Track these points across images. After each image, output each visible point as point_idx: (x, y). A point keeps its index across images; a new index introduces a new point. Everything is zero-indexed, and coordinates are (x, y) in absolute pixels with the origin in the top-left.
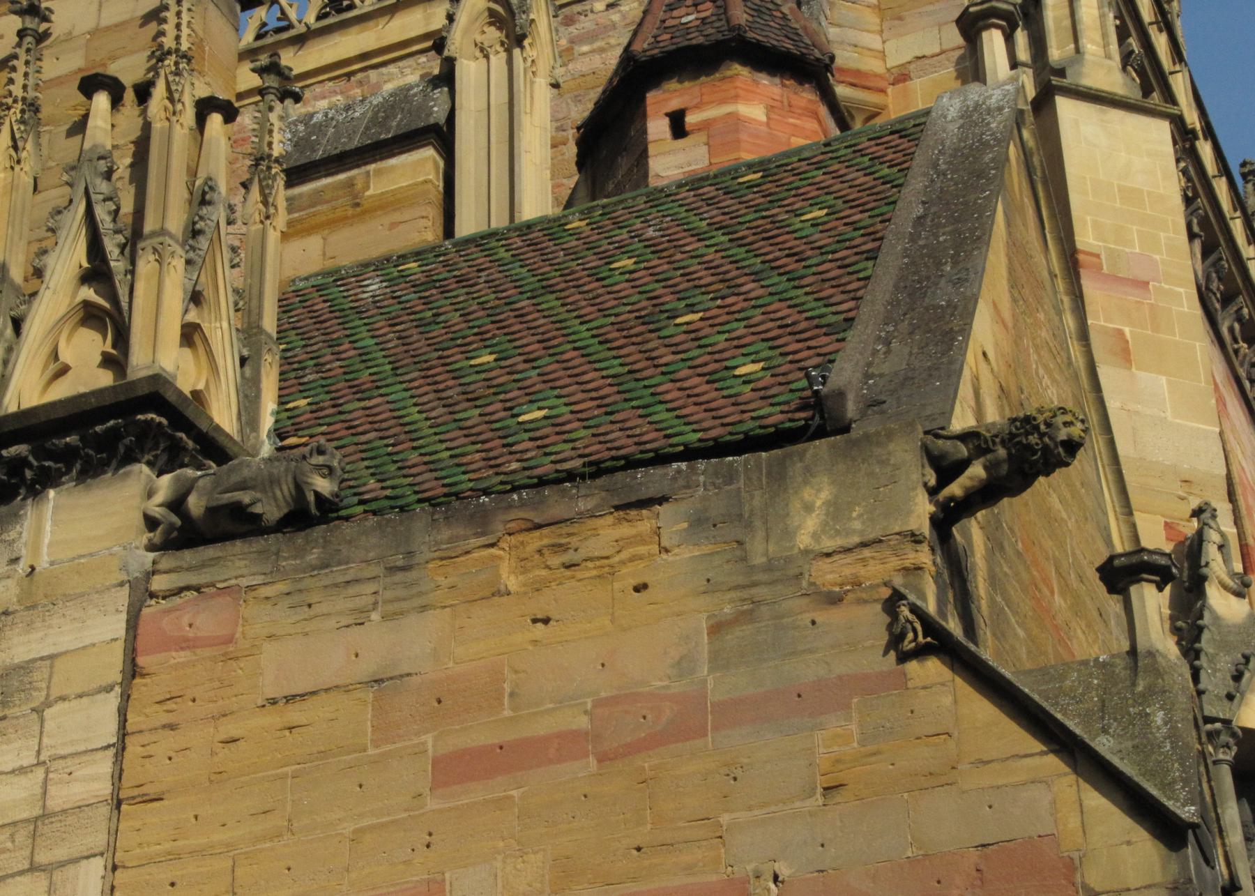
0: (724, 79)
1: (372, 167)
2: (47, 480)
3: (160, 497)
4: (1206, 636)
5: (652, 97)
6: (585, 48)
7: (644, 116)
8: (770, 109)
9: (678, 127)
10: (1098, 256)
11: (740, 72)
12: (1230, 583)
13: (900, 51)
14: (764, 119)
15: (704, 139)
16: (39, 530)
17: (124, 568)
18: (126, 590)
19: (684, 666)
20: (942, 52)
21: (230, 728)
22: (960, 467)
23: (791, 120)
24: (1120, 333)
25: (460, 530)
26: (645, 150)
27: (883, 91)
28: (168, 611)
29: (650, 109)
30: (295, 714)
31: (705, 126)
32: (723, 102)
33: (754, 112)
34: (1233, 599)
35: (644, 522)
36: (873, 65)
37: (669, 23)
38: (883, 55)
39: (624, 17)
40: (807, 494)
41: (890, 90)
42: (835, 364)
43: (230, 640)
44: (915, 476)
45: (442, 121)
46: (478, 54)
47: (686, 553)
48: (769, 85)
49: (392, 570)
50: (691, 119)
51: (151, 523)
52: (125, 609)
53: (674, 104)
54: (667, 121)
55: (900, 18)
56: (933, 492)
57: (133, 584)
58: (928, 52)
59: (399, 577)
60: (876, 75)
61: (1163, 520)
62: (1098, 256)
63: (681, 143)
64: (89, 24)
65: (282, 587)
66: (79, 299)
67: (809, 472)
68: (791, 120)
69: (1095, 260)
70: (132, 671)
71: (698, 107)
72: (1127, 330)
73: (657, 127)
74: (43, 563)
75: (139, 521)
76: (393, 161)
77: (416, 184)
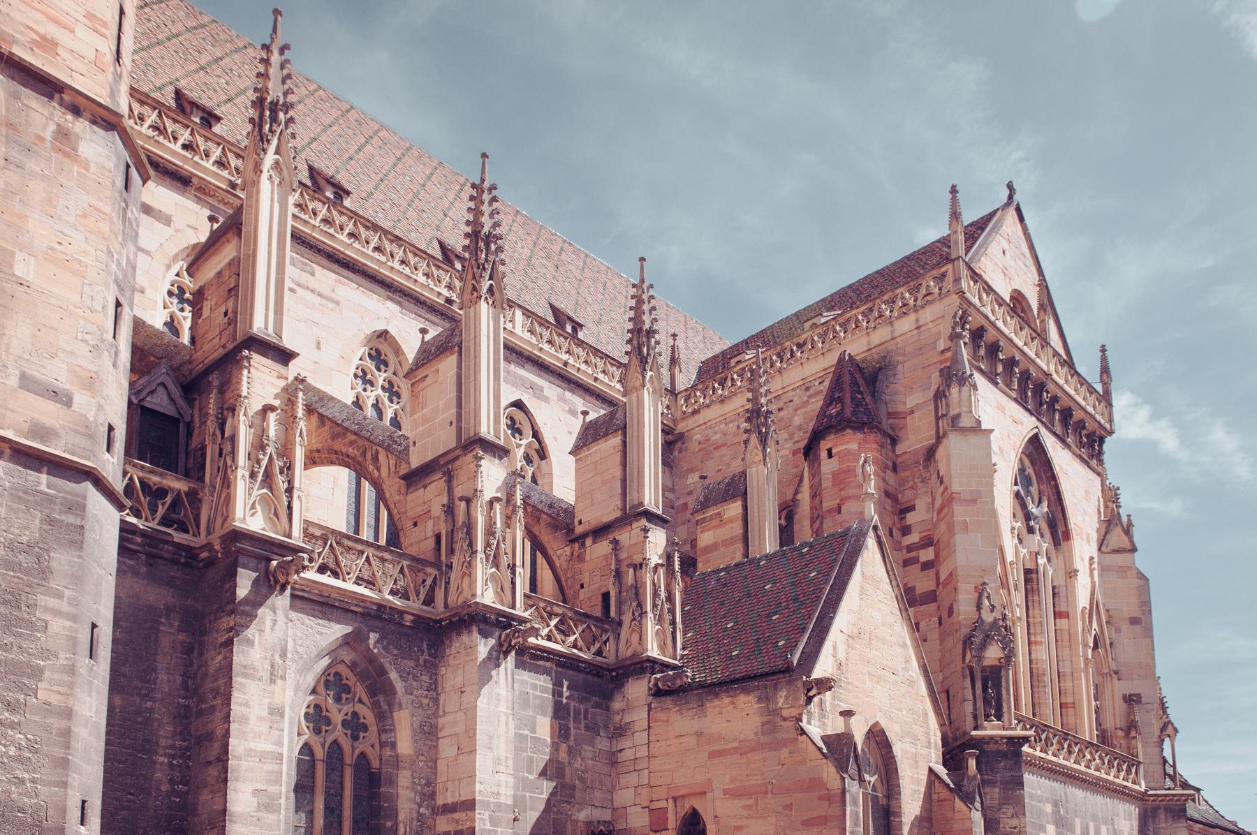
6: (813, 400)
8: (859, 444)
9: (830, 455)
19: (756, 734)
21: (669, 742)
24: (965, 520)
25: (712, 697)
30: (682, 740)
31: (839, 453)
43: (668, 721)
47: (756, 706)
49: (699, 706)
50: (834, 451)
51: (650, 689)
53: (829, 446)
65: (678, 708)
70: (649, 727)
72: (968, 519)
73: (824, 454)
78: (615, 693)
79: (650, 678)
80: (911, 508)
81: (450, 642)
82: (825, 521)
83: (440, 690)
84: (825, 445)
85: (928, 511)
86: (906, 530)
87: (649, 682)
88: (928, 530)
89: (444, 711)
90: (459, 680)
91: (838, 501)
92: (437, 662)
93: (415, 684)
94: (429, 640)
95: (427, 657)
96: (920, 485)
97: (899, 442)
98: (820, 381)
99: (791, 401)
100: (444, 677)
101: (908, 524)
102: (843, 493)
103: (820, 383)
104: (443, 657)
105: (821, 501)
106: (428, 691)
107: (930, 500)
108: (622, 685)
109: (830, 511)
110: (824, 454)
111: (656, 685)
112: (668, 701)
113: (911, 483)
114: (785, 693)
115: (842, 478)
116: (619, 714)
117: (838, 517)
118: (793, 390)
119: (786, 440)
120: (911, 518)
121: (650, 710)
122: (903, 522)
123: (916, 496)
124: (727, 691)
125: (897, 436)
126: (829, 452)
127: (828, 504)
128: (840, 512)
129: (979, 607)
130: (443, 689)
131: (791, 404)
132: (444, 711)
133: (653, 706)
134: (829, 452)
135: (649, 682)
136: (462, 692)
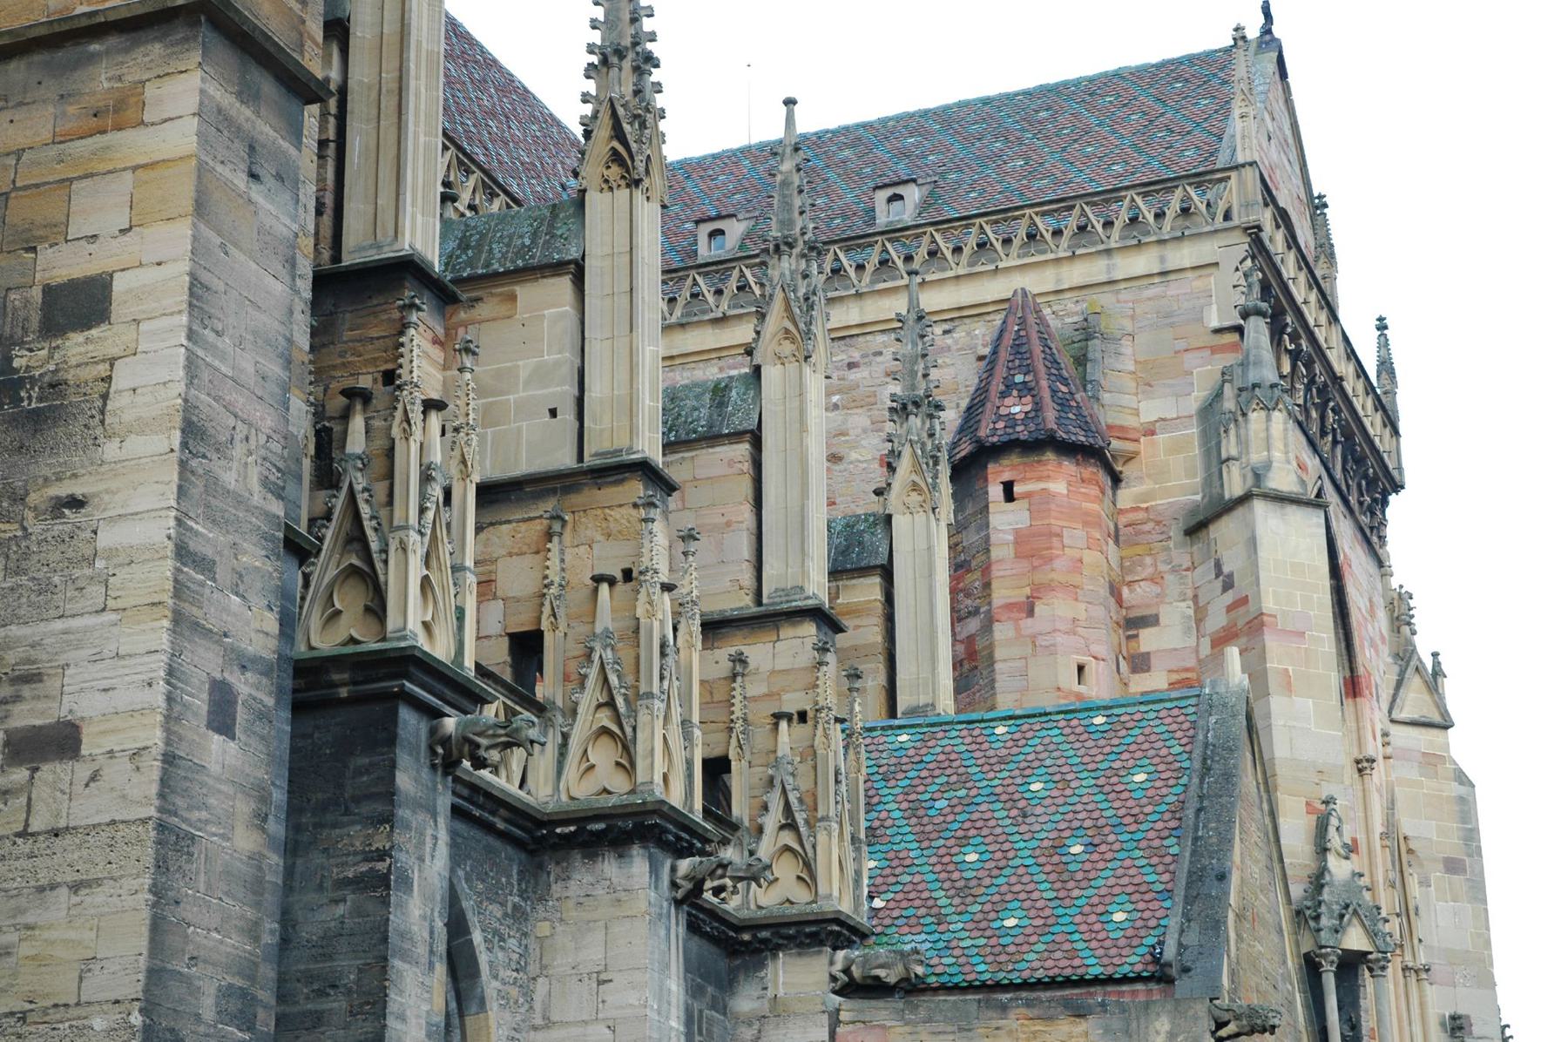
0: (1039, 462)
1: (841, 583)
2: (778, 947)
3: (839, 966)
4: (1326, 890)
5: (991, 467)
7: (986, 480)
9: (1009, 496)
10: (1275, 617)
11: (1050, 456)
12: (1342, 852)
13: (1151, 410)
14: (1065, 492)
15: (1027, 506)
16: (776, 975)
17: (824, 1003)
18: (826, 1016)
20: (1178, 418)
22: (1226, 1024)
23: (1083, 490)
24: (1286, 670)
26: (987, 507)
27: (1137, 441)
28: (851, 1032)
29: (990, 477)
31: (1028, 495)
32: (1040, 479)
33: (1059, 487)
34: (1344, 861)
35: (1082, 1026)
36: (1129, 421)
37: (1003, 411)
38: (1137, 413)
39: (956, 342)
40: (1158, 1025)
41: (1142, 439)
42: (1027, 289)
44: (1206, 1025)
45: (885, 562)
46: (906, 511)
48: (1069, 466)
49: (961, 1029)
50: (1017, 489)
51: (834, 978)
52: (827, 1025)
53: (1006, 477)
54: (1001, 487)
55: (1150, 386)
56: (1213, 1033)
57: (830, 1015)
58: (1169, 417)
59: (965, 1034)
60: (1134, 429)
61: (1304, 800)
62: (1275, 617)
63: (1010, 506)
64: (769, 667)
65: (908, 1029)
66: (780, 844)
67: (1158, 1014)
68: (1083, 490)
69: (1272, 619)
71: (1024, 480)
72: (1290, 668)
73: (995, 491)
74: (781, 993)
75: (826, 977)
76: (854, 582)
77: (870, 601)
78: (741, 977)
79: (832, 957)
80: (1149, 621)
81: (565, 870)
82: (997, 627)
83: (533, 969)
84: (998, 472)
85: (1187, 631)
86: (1140, 663)
87: (832, 963)
88: (1187, 670)
89: (546, 1018)
90: (592, 954)
91: (1027, 591)
92: (528, 909)
93: (500, 955)
94: (520, 863)
95: (517, 899)
96: (1169, 578)
97: (1123, 484)
98: (946, 326)
99: (880, 353)
100: (547, 942)
101: (1143, 649)
102: (1039, 577)
103: (946, 332)
104: (542, 899)
105: (987, 585)
106: (517, 970)
107: (1191, 612)
108: (761, 965)
109: (1010, 607)
110: (995, 491)
111: (847, 971)
112: (881, 1011)
113: (1150, 570)
114: (1167, 1027)
115: (1032, 547)
116: (750, 1024)
117: (1028, 625)
118: (883, 331)
119: (865, 431)
120: (1148, 640)
121: (835, 1021)
122: (1133, 644)
123: (1161, 597)
124: (1029, 1004)
125: (1121, 472)
126: (1008, 487)
127: (1002, 594)
128: (1031, 613)
129: (1322, 850)
130: (543, 967)
131: (879, 359)
132: (546, 1018)
133: (844, 1016)
134: (1008, 487)
135: (832, 963)
136: (600, 983)
